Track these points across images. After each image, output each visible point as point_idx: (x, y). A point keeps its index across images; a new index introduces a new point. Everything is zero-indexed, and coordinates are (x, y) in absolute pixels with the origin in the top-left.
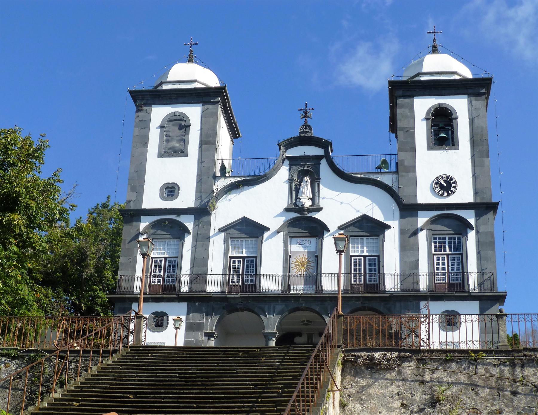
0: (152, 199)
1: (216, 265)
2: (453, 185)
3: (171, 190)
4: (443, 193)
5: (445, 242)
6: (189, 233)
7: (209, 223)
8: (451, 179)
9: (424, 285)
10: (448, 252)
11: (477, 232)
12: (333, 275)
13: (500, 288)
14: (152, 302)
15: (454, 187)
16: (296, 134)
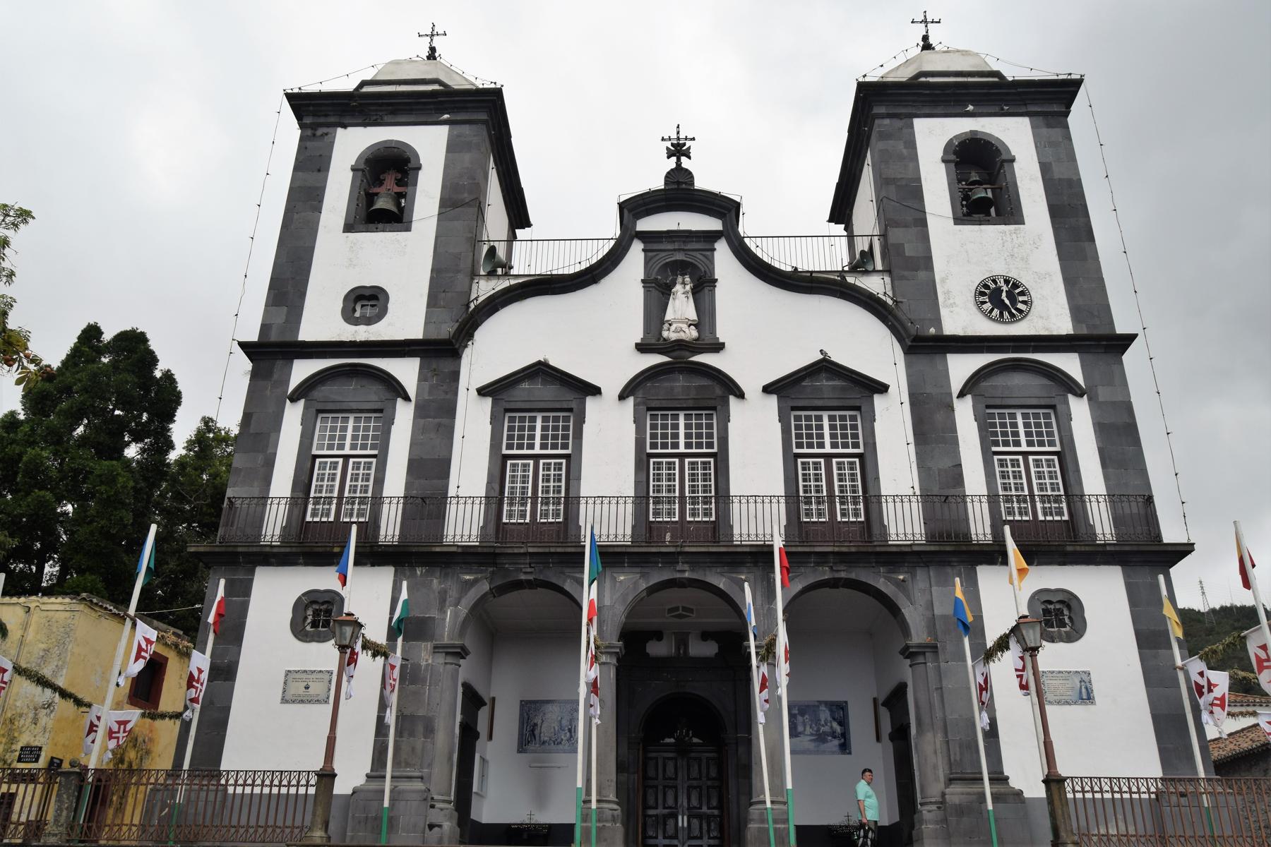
0: (321, 320)
1: (469, 474)
2: (1021, 298)
4: (1001, 315)
5: (1014, 425)
7: (455, 376)
8: (1016, 286)
9: (980, 528)
10: (1024, 448)
12: (759, 500)
13: (1171, 534)
14: (306, 564)
15: (1024, 302)
16: (659, 184)
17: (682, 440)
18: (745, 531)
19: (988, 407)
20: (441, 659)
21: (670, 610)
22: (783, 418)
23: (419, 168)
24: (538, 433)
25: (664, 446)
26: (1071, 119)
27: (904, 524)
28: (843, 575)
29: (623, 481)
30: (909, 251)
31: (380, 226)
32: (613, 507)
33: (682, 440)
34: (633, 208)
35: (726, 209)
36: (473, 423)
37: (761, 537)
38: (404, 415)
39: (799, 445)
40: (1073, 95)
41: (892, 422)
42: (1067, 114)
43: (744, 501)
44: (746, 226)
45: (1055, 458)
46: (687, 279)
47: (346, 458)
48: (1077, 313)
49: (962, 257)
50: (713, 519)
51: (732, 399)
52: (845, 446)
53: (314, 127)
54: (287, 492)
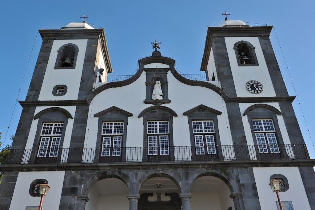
0: (46, 94)
1: (91, 140)
2: (260, 87)
4: (254, 92)
6: (72, 118)
8: (258, 83)
9: (253, 155)
11: (284, 117)
12: (183, 147)
14: (36, 171)
15: (260, 88)
16: (150, 55)
17: (158, 130)
18: (179, 157)
19: (252, 119)
20: (79, 202)
21: (155, 185)
22: (190, 123)
23: (78, 51)
24: (113, 128)
25: (153, 132)
26: (270, 37)
27: (229, 155)
28: (210, 171)
29: (140, 143)
30: (225, 74)
31: (65, 67)
32: (137, 150)
33: (158, 130)
34: (143, 62)
35: (171, 62)
36: (92, 124)
37: (184, 159)
38: (71, 123)
39: (195, 131)
40: (270, 31)
43: (178, 148)
44: (177, 67)
45: (274, 134)
46: (159, 81)
47: (51, 137)
48: (276, 91)
49: (241, 75)
50: (168, 154)
51: (174, 118)
52: (209, 131)
53: (47, 40)
54: (31, 147)
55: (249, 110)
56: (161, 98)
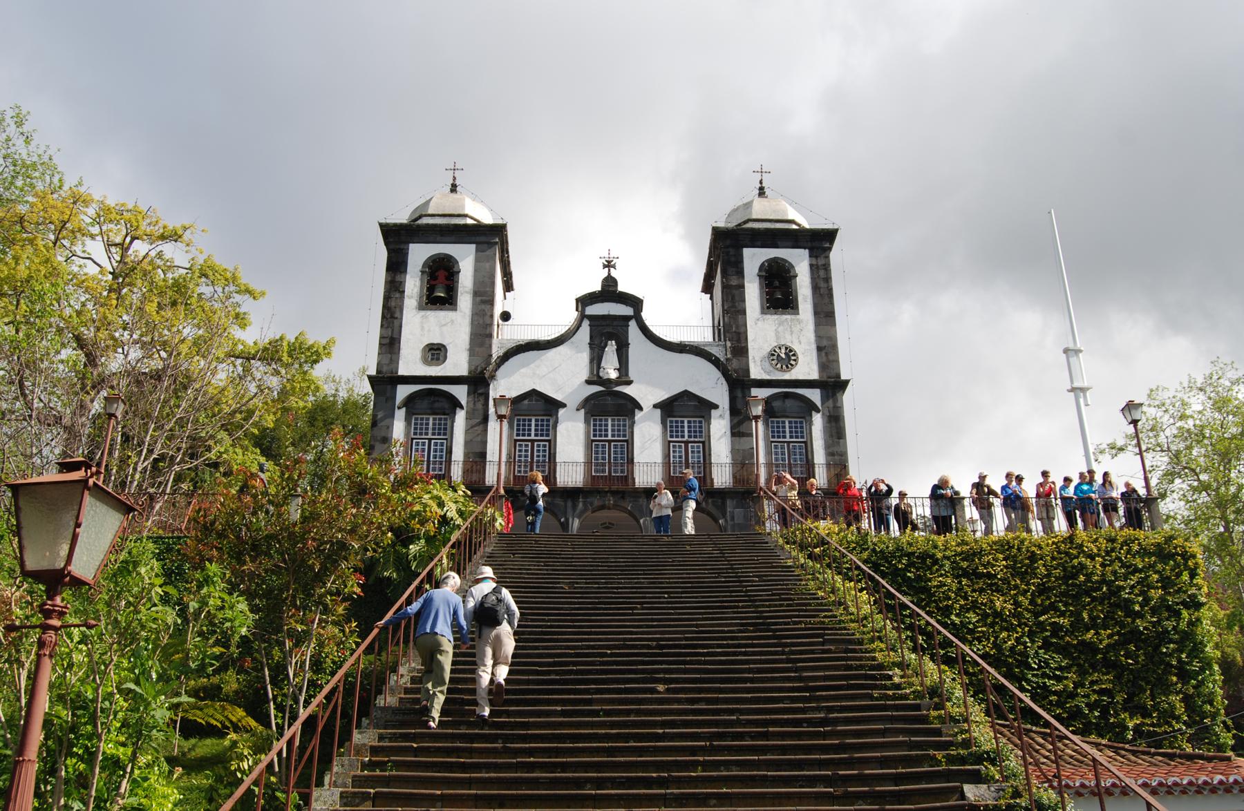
3: (436, 352)
6: (462, 407)
16: (597, 287)
17: (610, 433)
24: (533, 428)
27: (722, 477)
33: (610, 433)
34: (584, 301)
35: (636, 303)
41: (719, 426)
42: (830, 249)
47: (430, 440)
48: (823, 367)
49: (763, 332)
55: (768, 402)
56: (613, 375)
